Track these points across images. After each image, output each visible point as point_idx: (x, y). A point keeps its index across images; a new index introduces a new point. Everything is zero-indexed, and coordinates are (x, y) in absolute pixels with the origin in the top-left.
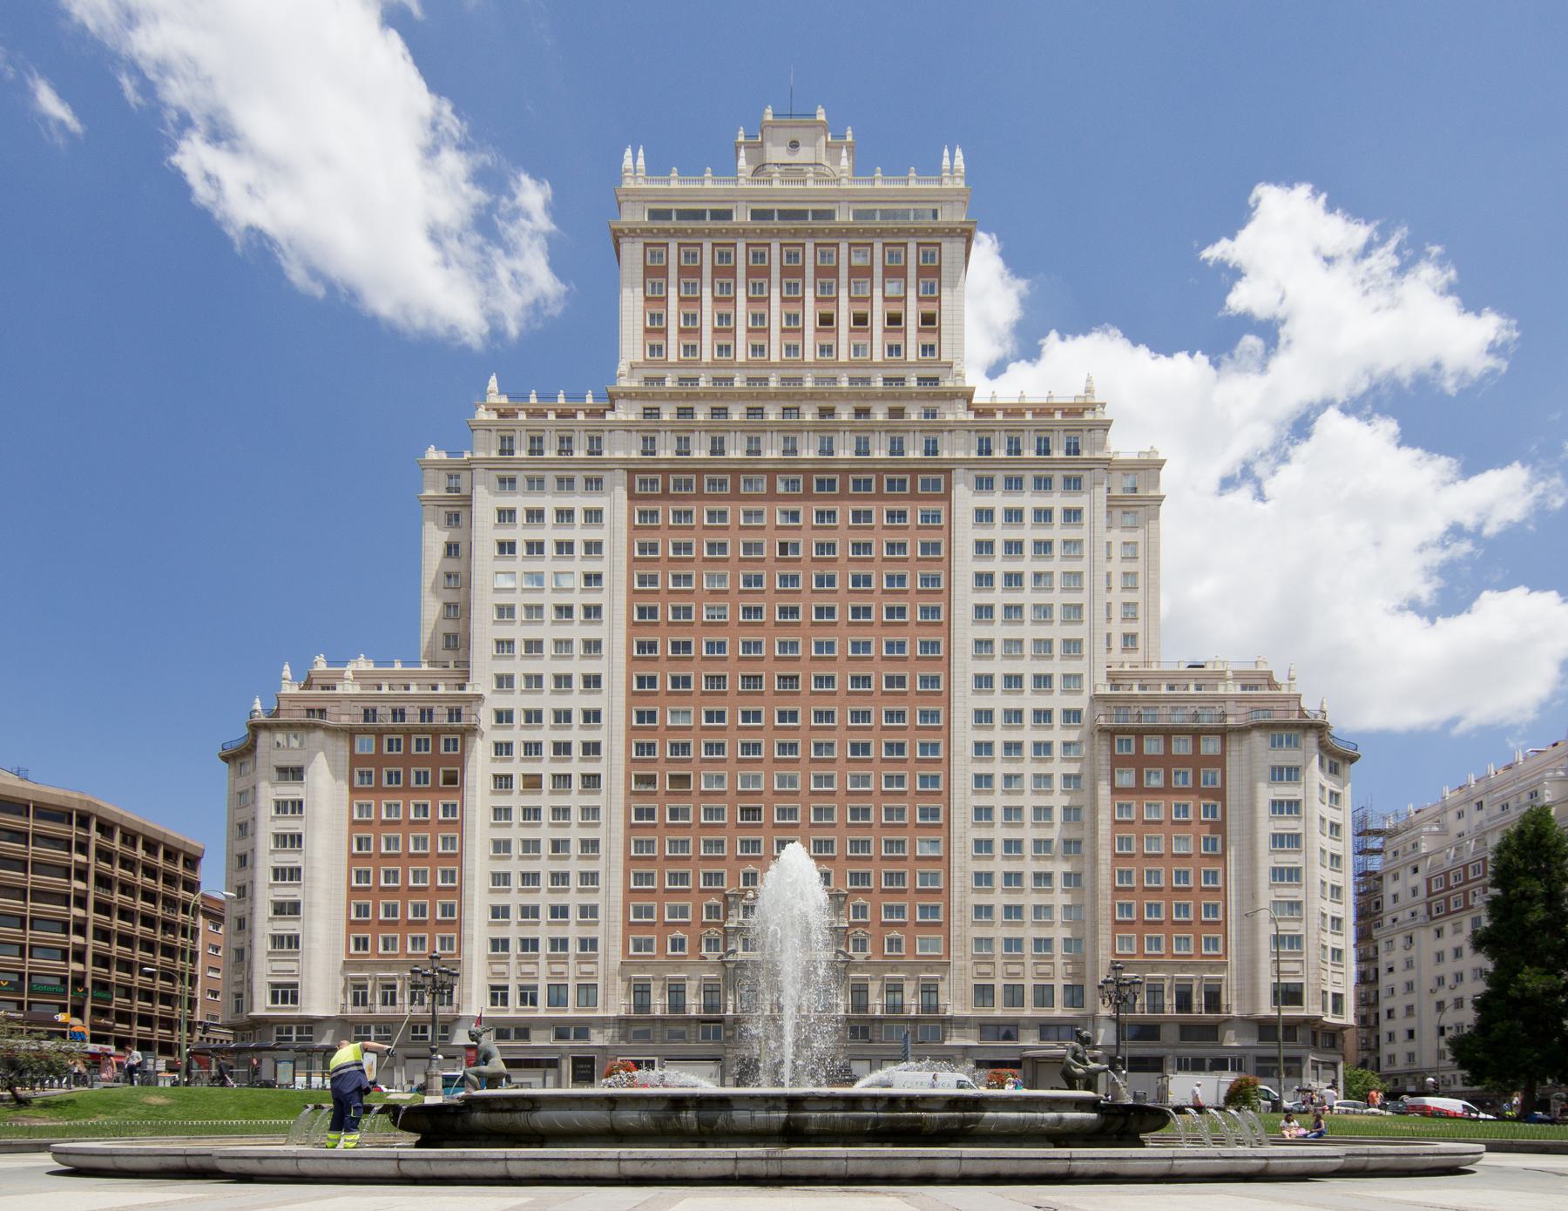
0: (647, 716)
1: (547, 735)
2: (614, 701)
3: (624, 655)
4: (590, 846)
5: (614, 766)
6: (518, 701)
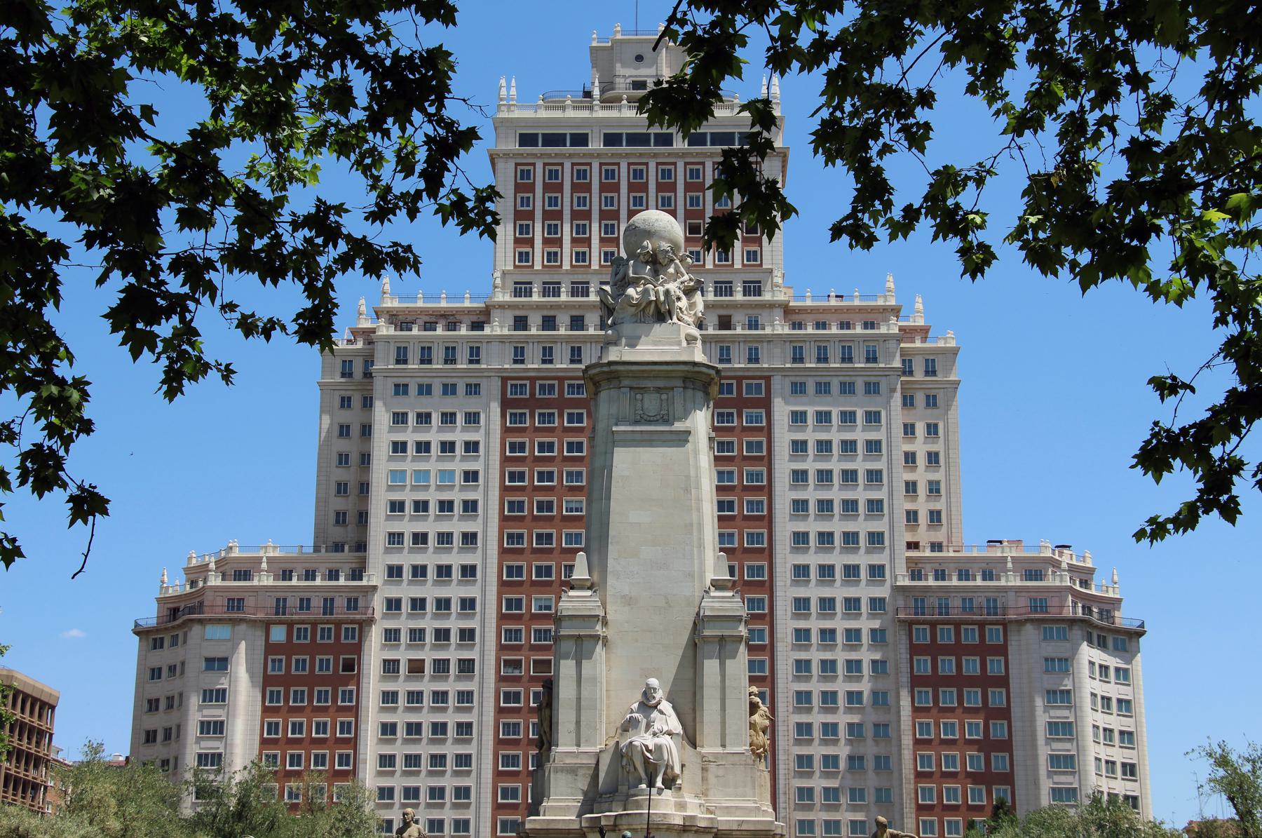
2: (487, 591)
3: (496, 547)
4: (465, 728)
5: (486, 653)
6: (406, 591)
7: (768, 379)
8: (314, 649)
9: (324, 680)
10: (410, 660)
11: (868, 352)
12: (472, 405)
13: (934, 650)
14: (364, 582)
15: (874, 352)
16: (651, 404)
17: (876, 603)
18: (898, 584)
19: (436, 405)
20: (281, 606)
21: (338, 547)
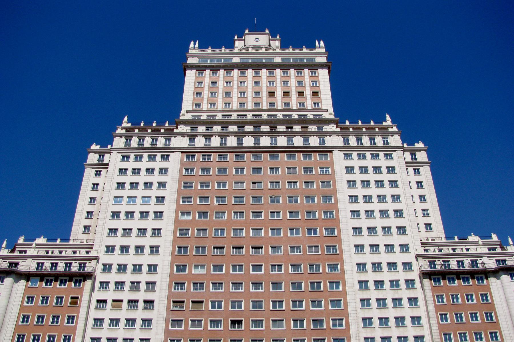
0: (181, 268)
1: (128, 277)
6: (116, 259)
7: (331, 152)
10: (114, 301)
11: (384, 141)
12: (164, 165)
14: (92, 254)
15: (387, 141)
17: (407, 266)
18: (418, 253)
19: (144, 164)
20: (40, 265)
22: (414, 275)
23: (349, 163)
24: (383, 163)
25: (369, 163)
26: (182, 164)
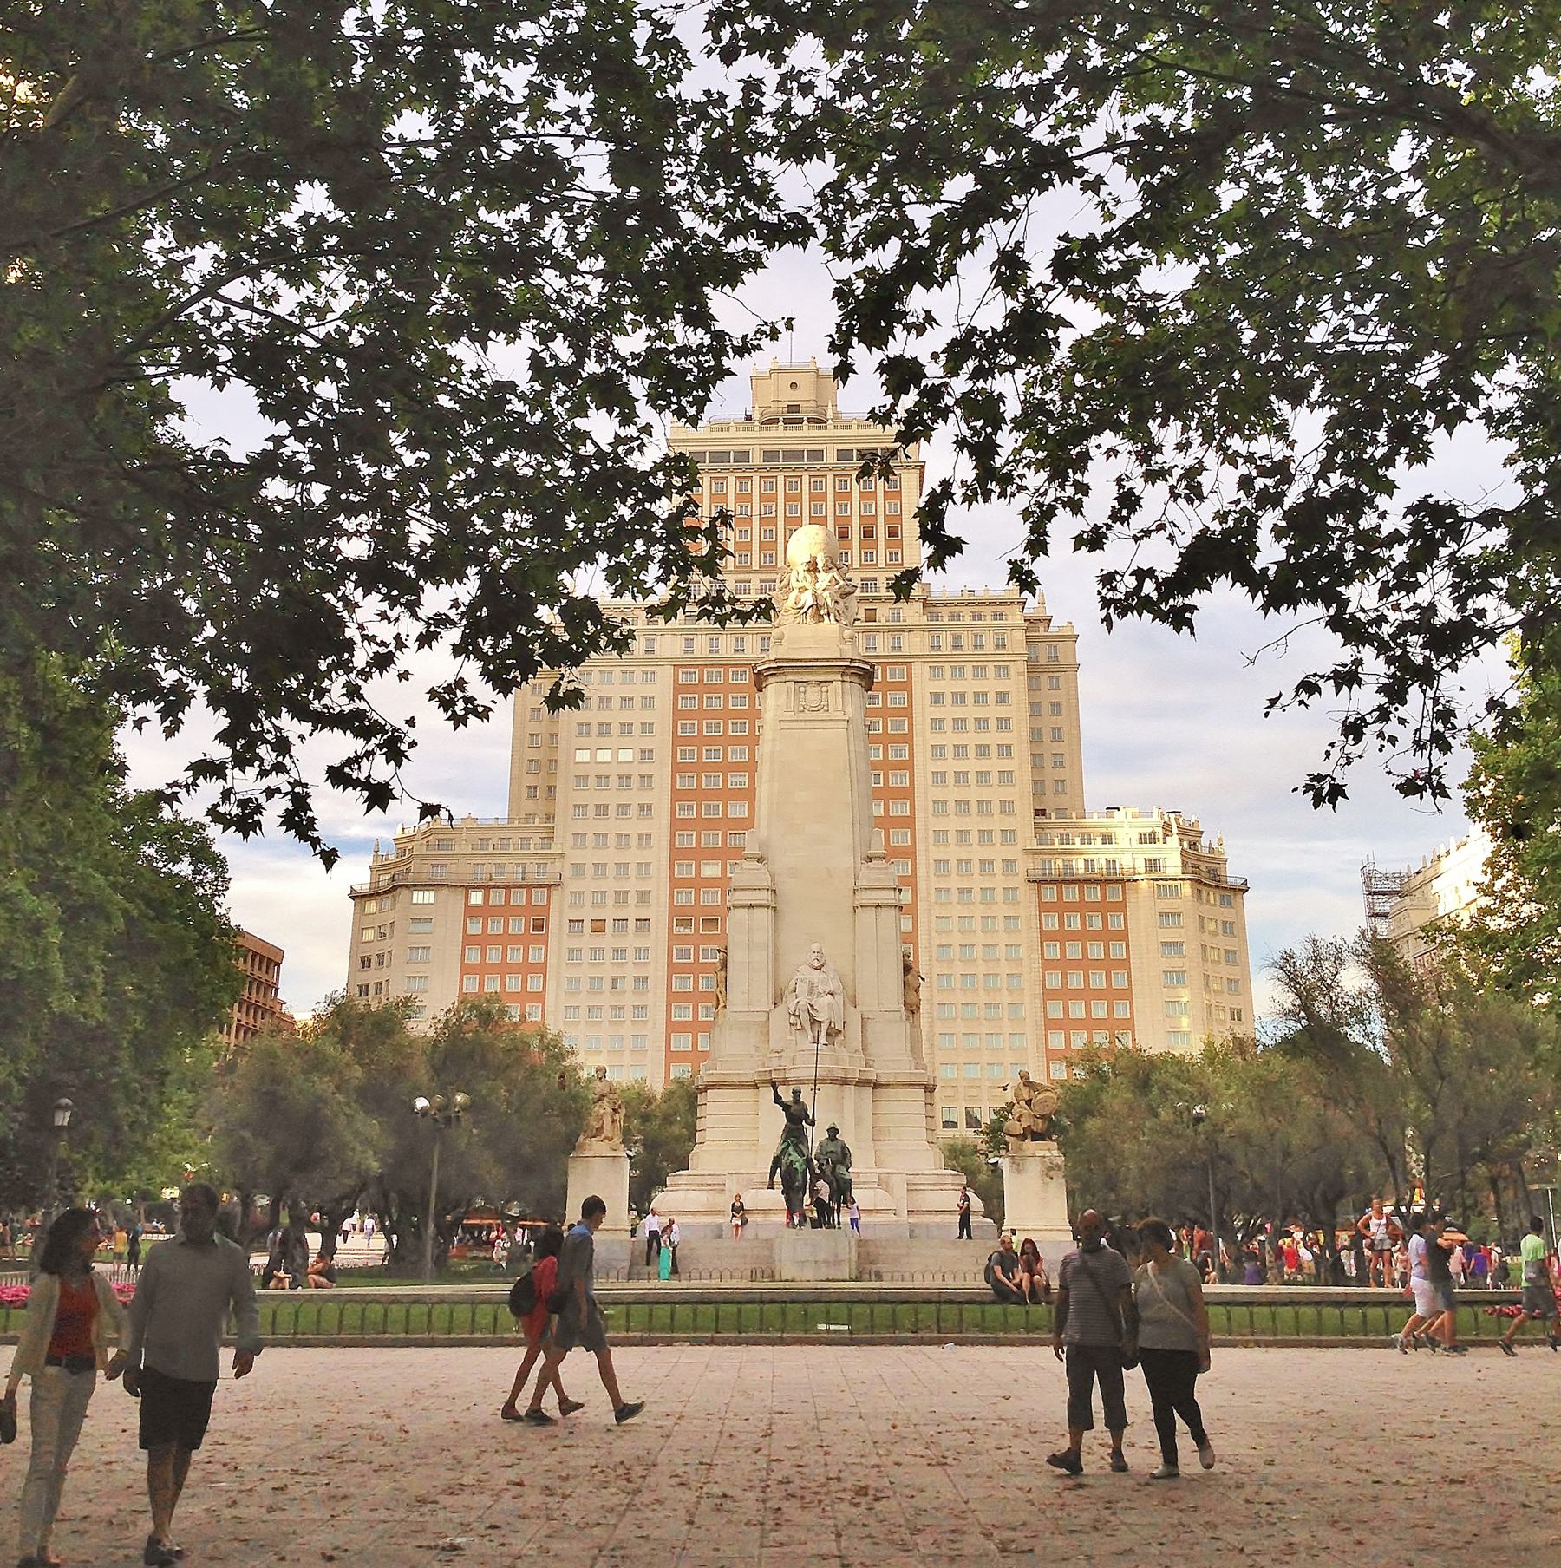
1: (610, 885)
8: (507, 911)
9: (516, 939)
13: (1061, 907)
14: (555, 849)
16: (812, 695)
21: (530, 817)
22: (1018, 881)
23: (937, 686)
24: (991, 685)
25: (969, 685)
26: (678, 689)
